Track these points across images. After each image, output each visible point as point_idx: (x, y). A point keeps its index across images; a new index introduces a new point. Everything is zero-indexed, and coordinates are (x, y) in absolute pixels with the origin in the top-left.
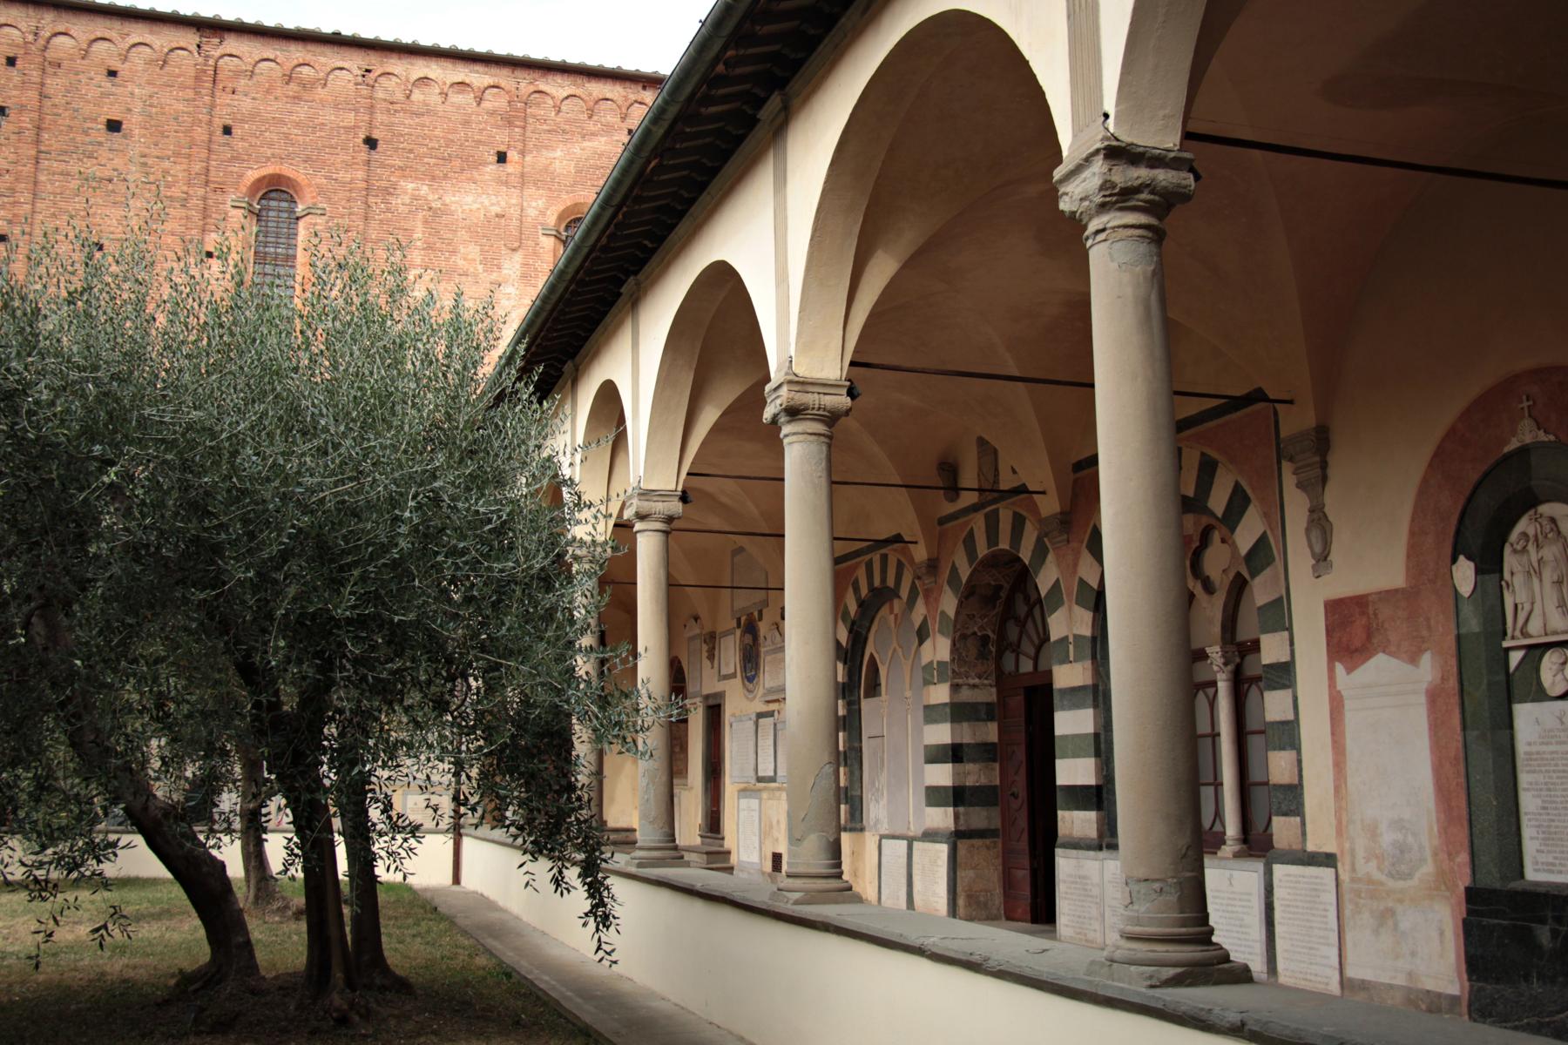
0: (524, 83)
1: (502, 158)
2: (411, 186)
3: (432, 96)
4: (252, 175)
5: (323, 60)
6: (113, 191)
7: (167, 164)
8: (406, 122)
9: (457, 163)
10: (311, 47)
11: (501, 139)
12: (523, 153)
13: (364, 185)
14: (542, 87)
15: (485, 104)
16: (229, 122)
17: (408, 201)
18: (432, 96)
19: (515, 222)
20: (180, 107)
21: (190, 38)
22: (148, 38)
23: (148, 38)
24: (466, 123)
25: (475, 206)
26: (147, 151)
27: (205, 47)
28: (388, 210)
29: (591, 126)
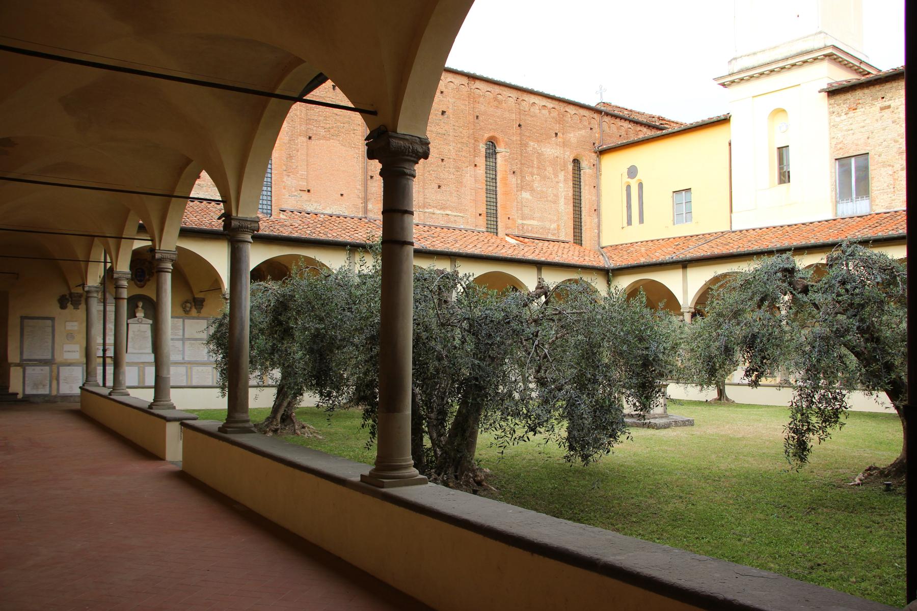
0: (561, 107)
1: (556, 134)
2: (532, 144)
3: (535, 110)
4: (487, 136)
5: (504, 93)
6: (446, 139)
7: (461, 130)
8: (529, 119)
9: (544, 136)
10: (502, 88)
11: (557, 128)
12: (563, 134)
13: (519, 142)
14: (567, 110)
15: (551, 115)
16: (478, 114)
17: (531, 150)
18: (535, 110)
19: (562, 160)
20: (463, 107)
21: (465, 80)
22: (453, 80)
23: (453, 80)
24: (546, 121)
25: (550, 153)
26: (455, 124)
27: (470, 85)
28: (526, 153)
29: (581, 126)
